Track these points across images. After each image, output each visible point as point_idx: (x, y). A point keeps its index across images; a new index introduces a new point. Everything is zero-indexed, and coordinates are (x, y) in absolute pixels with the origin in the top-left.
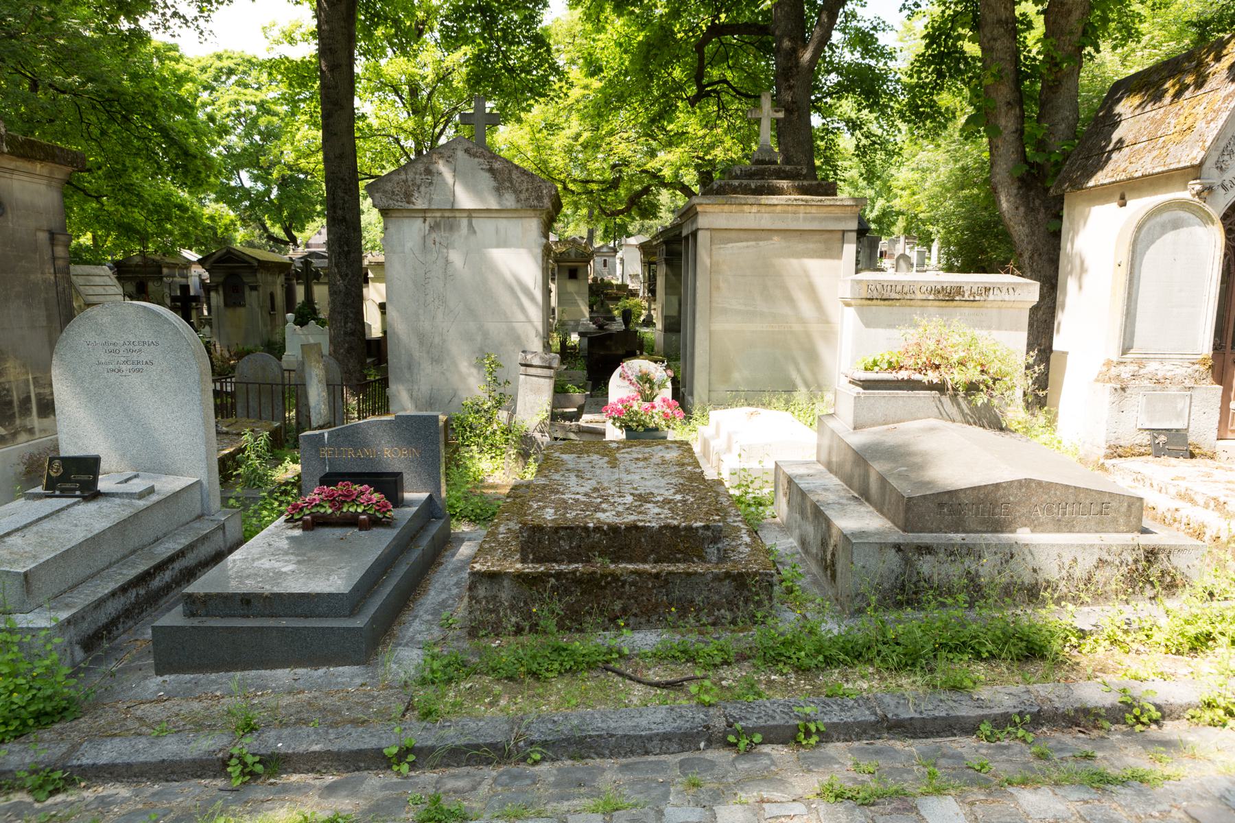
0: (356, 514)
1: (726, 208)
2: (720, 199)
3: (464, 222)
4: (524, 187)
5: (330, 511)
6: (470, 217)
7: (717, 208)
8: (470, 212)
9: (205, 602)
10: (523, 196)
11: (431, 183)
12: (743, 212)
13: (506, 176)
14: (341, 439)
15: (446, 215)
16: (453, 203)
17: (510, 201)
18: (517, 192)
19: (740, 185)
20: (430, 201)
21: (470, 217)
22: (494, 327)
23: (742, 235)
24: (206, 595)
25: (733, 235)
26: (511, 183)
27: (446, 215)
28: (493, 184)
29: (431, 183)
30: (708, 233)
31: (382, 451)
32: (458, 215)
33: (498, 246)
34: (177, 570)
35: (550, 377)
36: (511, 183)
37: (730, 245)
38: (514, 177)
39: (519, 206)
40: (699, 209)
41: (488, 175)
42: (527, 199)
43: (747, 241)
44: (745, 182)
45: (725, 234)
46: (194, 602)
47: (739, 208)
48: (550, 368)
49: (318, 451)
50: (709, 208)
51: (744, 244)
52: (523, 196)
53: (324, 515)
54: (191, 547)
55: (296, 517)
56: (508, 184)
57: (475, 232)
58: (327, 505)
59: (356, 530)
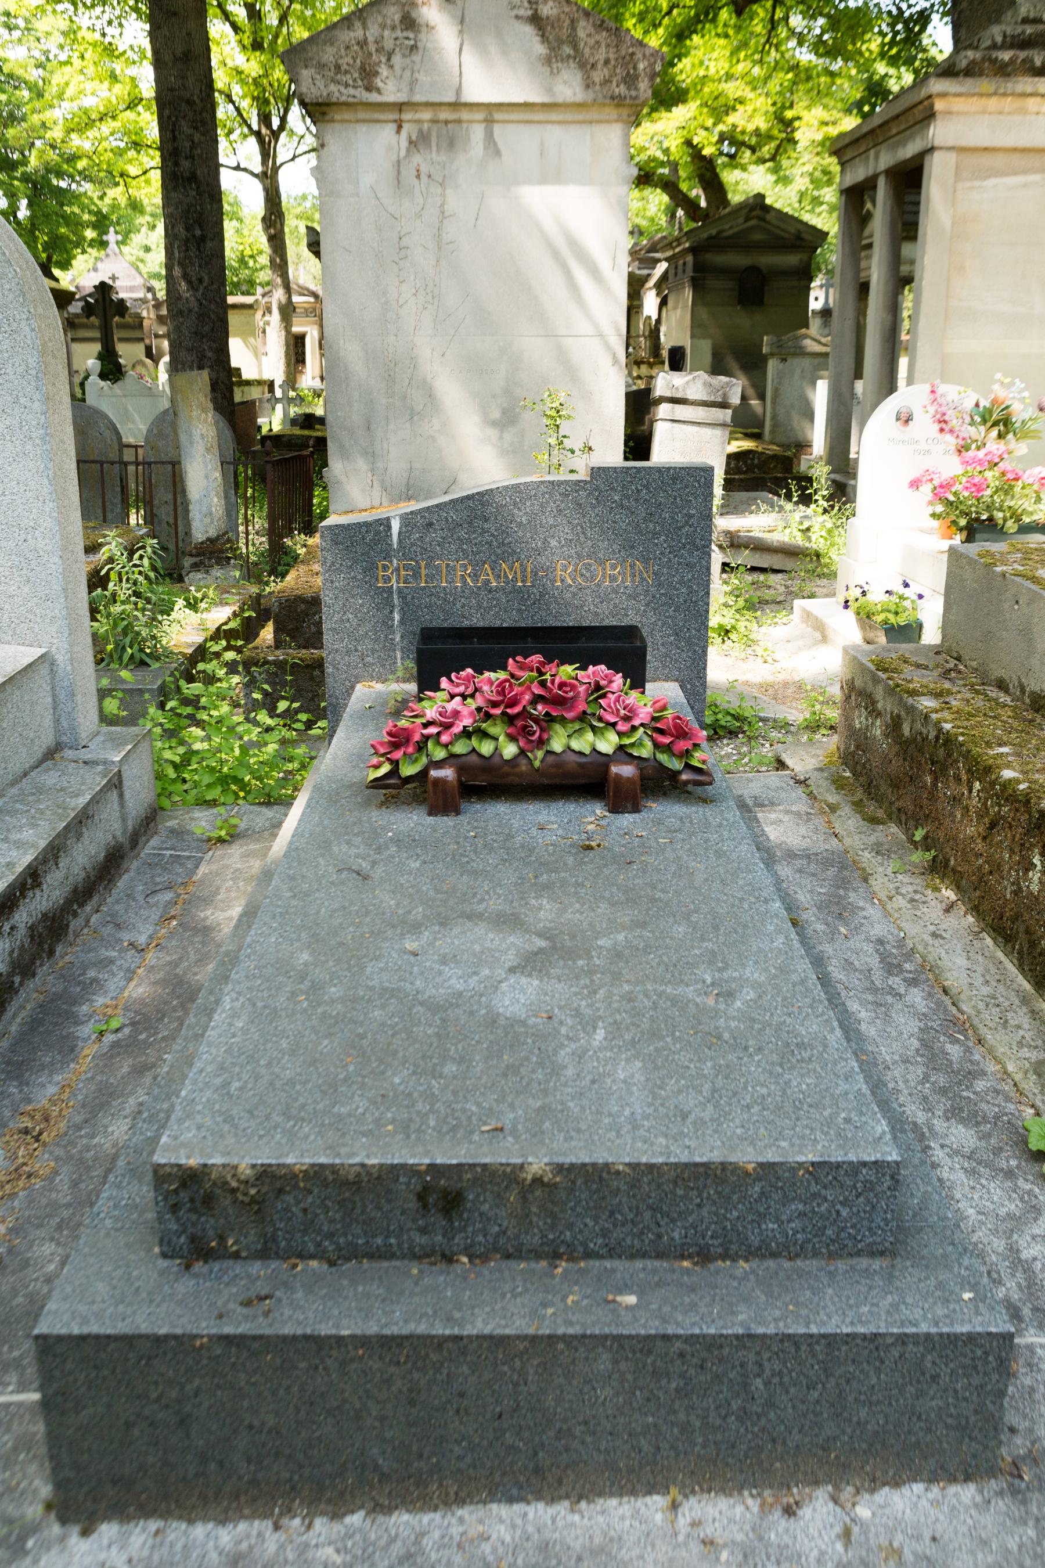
0: (603, 761)
1: (993, 103)
2: (985, 84)
3: (478, 132)
4: (601, 55)
5: (510, 750)
6: (489, 122)
7: (973, 104)
8: (491, 111)
9: (257, 1207)
10: (598, 76)
11: (414, 48)
12: (1023, 111)
13: (564, 33)
14: (434, 535)
15: (443, 115)
16: (459, 91)
17: (569, 86)
18: (586, 66)
19: (1012, 61)
20: (413, 83)
21: (489, 122)
22: (534, 349)
23: (1017, 160)
24: (265, 1174)
25: (1000, 160)
26: (575, 47)
27: (443, 115)
28: (540, 49)
29: (414, 48)
30: (952, 157)
31: (550, 570)
32: (465, 115)
33: (543, 181)
34: (22, 931)
35: (724, 425)
36: (575, 47)
37: (992, 182)
38: (581, 34)
39: (589, 96)
40: (939, 105)
41: (529, 30)
42: (607, 82)
43: (1025, 172)
44: (1022, 55)
45: (986, 160)
46: (209, 1200)
47: (1019, 103)
48: (723, 405)
49: (370, 569)
50: (958, 105)
51: (1020, 179)
52: (598, 76)
53: (490, 765)
54: (53, 852)
55: (408, 770)
56: (568, 50)
57: (498, 153)
58: (497, 729)
59: (599, 809)
